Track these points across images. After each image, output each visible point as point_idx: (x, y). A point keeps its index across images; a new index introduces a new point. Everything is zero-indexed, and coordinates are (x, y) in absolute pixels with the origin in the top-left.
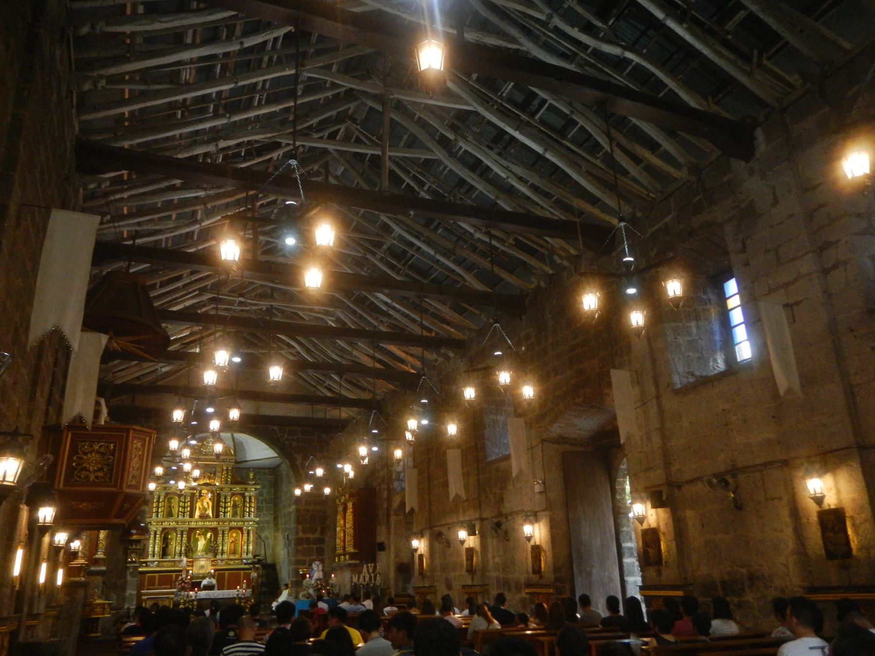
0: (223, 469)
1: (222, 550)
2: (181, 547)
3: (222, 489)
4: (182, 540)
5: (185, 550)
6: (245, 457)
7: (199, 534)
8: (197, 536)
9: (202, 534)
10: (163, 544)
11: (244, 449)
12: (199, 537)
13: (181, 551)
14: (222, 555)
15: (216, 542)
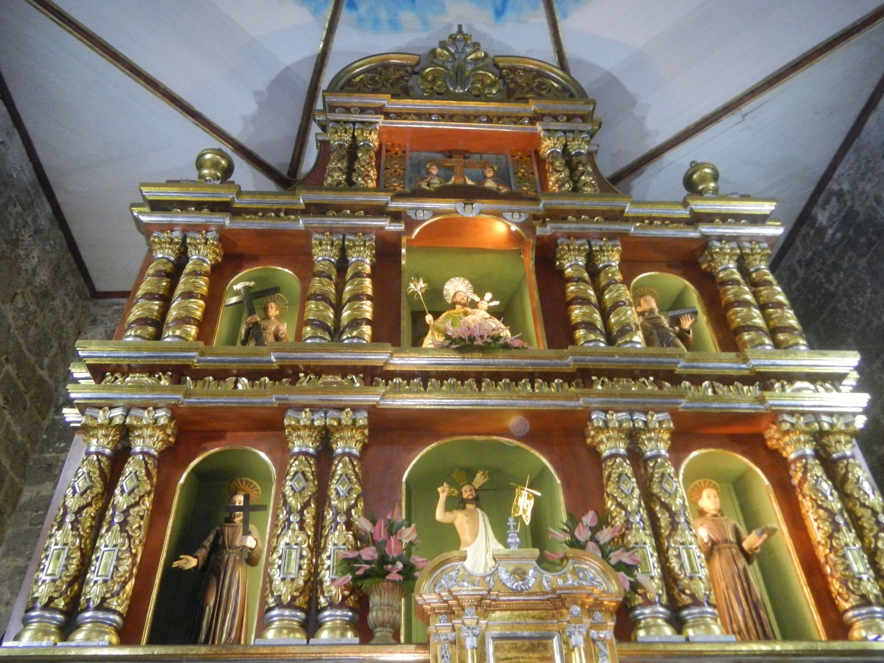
0: (541, 162)
1: (669, 578)
2: (317, 549)
3: (558, 216)
4: (321, 498)
5: (348, 564)
6: (645, 135)
7: (456, 503)
8: (440, 514)
9: (477, 501)
10: (182, 546)
11: (631, 101)
12: (460, 520)
13: (313, 584)
14: (678, 623)
15: (604, 519)
